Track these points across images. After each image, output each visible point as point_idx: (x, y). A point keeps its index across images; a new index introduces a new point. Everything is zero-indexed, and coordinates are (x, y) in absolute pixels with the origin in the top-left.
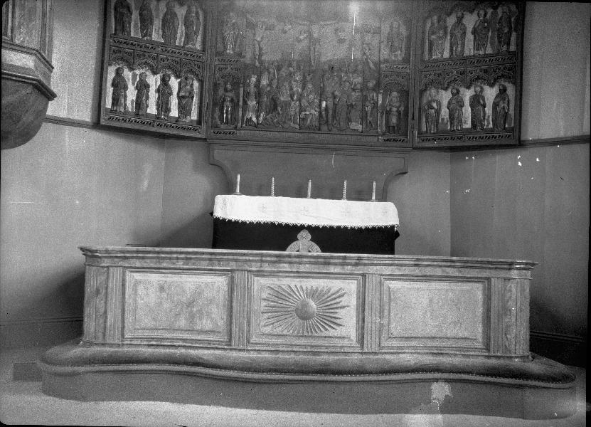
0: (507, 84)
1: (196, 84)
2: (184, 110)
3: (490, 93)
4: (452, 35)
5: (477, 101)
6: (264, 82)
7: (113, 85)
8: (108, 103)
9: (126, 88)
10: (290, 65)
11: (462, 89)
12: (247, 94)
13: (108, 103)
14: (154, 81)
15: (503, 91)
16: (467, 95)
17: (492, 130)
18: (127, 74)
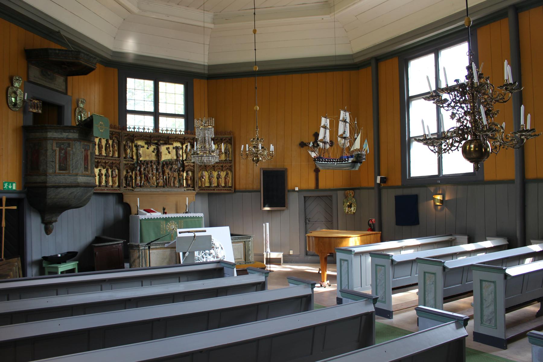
0: (229, 172)
1: (117, 171)
2: (113, 182)
3: (223, 174)
5: (219, 177)
6: (142, 169)
11: (213, 172)
12: (136, 174)
14: (104, 171)
15: (227, 174)
16: (215, 174)
17: (224, 187)
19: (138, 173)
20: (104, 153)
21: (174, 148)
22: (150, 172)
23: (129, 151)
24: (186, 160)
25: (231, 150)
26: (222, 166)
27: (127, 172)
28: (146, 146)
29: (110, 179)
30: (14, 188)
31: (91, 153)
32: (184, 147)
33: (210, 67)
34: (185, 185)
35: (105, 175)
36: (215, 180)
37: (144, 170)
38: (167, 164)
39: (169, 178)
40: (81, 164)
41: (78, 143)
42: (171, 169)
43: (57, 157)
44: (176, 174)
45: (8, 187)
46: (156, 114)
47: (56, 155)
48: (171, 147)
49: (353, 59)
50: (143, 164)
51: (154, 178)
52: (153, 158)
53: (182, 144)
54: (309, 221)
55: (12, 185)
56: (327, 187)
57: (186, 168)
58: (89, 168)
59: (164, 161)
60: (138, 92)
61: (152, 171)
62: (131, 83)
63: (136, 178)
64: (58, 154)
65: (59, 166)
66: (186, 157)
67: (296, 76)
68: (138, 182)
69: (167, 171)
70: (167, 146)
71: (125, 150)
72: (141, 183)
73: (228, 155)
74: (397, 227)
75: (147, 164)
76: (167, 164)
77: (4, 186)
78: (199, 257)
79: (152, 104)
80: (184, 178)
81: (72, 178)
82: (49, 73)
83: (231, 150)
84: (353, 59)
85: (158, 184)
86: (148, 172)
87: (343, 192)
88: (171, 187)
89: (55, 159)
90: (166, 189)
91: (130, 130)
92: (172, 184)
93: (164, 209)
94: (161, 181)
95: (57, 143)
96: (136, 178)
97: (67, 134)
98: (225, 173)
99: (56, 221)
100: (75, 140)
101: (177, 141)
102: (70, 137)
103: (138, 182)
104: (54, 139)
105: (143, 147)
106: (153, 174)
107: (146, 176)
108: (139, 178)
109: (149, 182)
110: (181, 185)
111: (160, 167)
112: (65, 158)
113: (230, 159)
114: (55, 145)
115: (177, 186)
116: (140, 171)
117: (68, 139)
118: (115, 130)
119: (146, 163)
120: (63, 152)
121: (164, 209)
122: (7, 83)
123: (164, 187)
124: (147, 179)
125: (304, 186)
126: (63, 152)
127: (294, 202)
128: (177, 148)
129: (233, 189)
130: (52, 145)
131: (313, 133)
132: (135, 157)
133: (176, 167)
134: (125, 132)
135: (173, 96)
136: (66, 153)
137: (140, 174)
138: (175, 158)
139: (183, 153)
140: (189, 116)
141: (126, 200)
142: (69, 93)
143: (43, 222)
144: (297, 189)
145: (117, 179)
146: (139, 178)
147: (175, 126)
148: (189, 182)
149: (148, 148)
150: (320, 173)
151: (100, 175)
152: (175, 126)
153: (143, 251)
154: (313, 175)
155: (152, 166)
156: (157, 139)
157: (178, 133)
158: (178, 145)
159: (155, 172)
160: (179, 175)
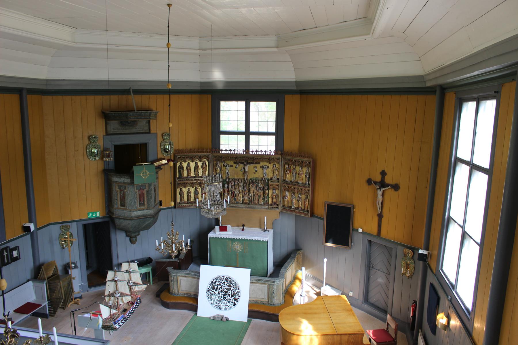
6: (230, 187)
8: (178, 201)
9: (184, 194)
10: (238, 180)
13: (178, 201)
14: (192, 190)
18: (184, 189)
19: (226, 189)
20: (192, 174)
23: (218, 170)
24: (272, 179)
30: (98, 215)
31: (147, 191)
32: (271, 166)
33: (297, 83)
34: (270, 202)
37: (232, 188)
38: (253, 182)
39: (254, 195)
40: (135, 202)
42: (256, 187)
43: (119, 196)
44: (261, 192)
45: (92, 216)
46: (247, 133)
49: (425, 82)
54: (373, 267)
57: (270, 187)
58: (146, 203)
59: (251, 179)
60: (231, 113)
62: (224, 105)
65: (121, 203)
66: (273, 175)
67: (371, 97)
69: (253, 189)
76: (253, 182)
77: (88, 215)
78: (216, 292)
80: (270, 195)
81: (128, 213)
84: (425, 82)
85: (243, 200)
86: (235, 189)
87: (403, 248)
88: (255, 204)
92: (256, 202)
93: (243, 226)
94: (246, 198)
99: (139, 234)
100: (128, 184)
101: (263, 161)
104: (116, 182)
105: (232, 166)
106: (239, 191)
107: (233, 193)
109: (235, 199)
110: (266, 203)
112: (124, 197)
115: (262, 203)
116: (228, 187)
117: (124, 183)
118: (203, 154)
120: (122, 192)
126: (122, 192)
127: (358, 243)
131: (381, 171)
133: (262, 186)
134: (215, 154)
135: (264, 114)
136: (124, 193)
137: (228, 191)
142: (153, 130)
143: (127, 236)
144: (360, 230)
147: (265, 145)
148: (274, 200)
150: (383, 219)
151: (189, 193)
152: (265, 145)
153: (175, 277)
154: (376, 219)
156: (247, 159)
160: (264, 193)
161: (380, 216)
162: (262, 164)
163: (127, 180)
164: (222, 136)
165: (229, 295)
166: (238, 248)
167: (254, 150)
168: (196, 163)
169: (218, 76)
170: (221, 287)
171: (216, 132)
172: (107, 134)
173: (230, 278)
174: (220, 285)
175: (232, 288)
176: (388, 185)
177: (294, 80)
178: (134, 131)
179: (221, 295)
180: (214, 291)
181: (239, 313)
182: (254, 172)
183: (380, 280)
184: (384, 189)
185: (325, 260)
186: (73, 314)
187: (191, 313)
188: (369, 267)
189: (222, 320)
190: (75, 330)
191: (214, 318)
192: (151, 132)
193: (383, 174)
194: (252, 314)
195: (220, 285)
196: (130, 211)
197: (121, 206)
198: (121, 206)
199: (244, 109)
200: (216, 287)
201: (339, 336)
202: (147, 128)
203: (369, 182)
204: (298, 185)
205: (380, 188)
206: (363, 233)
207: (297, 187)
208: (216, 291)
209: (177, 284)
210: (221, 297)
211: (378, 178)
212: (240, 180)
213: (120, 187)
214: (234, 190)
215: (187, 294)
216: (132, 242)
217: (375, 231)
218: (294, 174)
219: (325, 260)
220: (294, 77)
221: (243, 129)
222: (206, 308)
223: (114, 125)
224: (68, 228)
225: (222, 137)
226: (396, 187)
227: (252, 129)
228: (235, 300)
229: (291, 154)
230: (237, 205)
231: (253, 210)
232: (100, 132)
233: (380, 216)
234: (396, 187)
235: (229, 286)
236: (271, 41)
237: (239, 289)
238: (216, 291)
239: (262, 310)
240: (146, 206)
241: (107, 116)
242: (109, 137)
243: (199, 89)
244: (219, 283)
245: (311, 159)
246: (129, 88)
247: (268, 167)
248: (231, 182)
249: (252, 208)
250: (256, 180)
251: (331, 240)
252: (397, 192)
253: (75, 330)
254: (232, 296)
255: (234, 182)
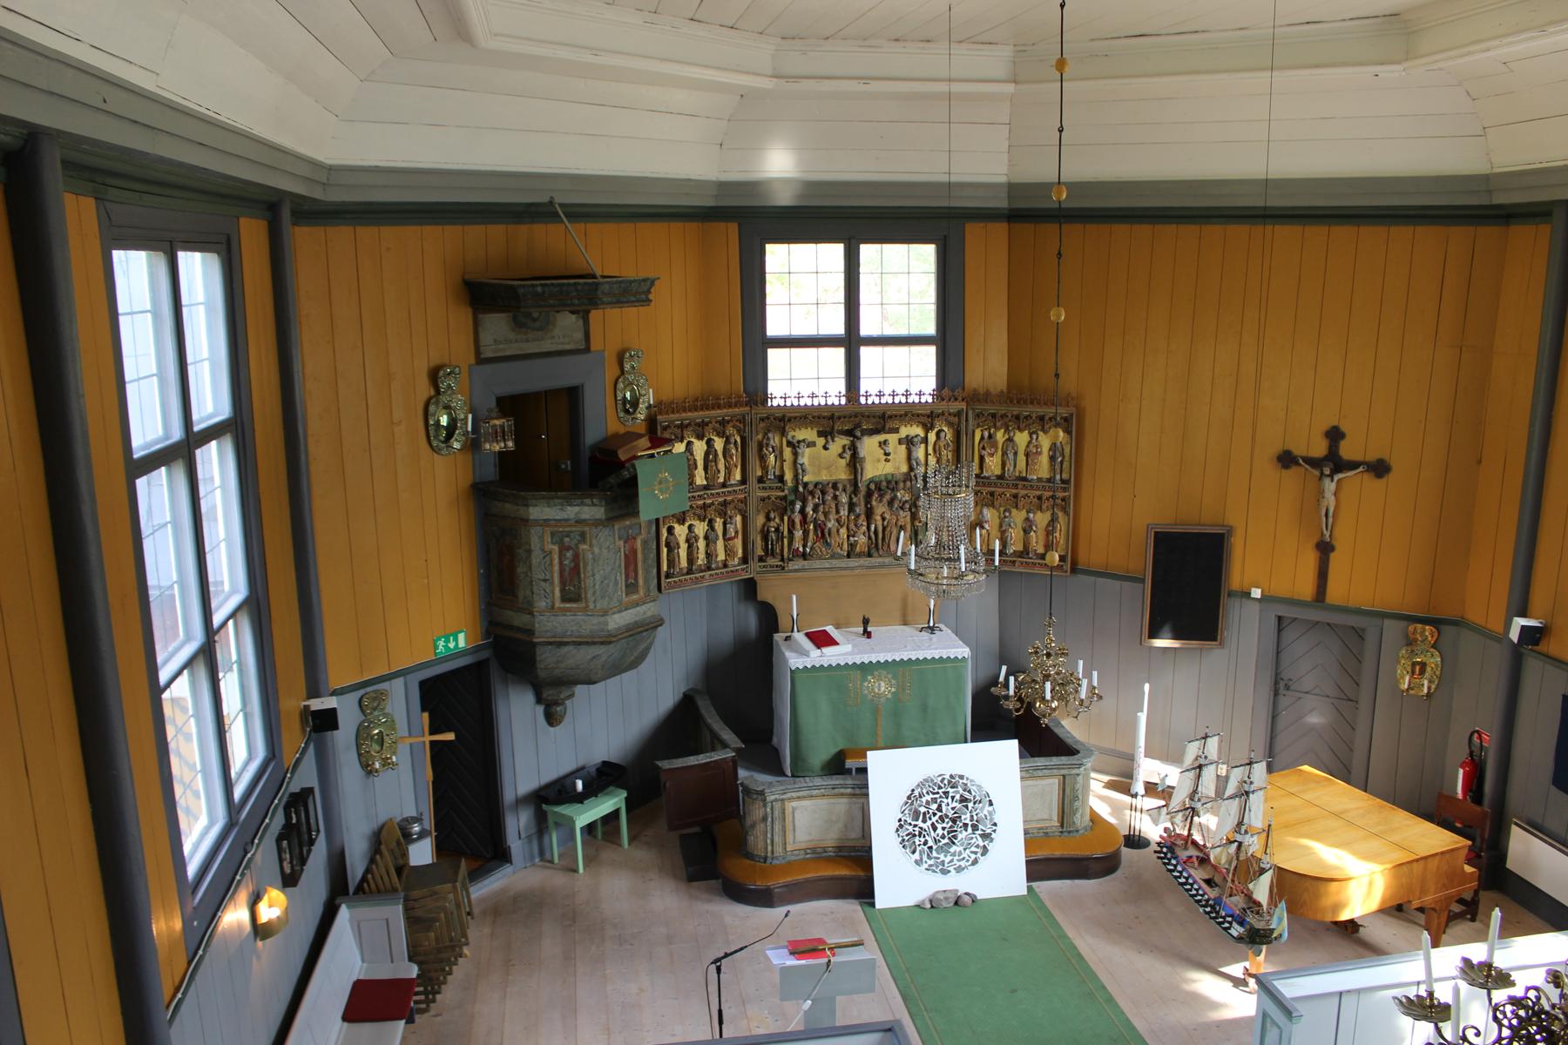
0: (1060, 514)
1: (739, 519)
2: (729, 552)
3: (1041, 519)
4: (1004, 454)
5: (1028, 528)
6: (809, 510)
7: (668, 545)
11: (1014, 511)
12: (792, 523)
14: (701, 528)
15: (1053, 520)
19: (797, 518)
21: (900, 442)
22: (833, 516)
25: (1067, 451)
26: (1039, 498)
27: (768, 519)
28: (821, 441)
29: (720, 544)
32: (932, 437)
33: (1013, 188)
35: (706, 538)
36: (1015, 535)
37: (815, 510)
40: (616, 583)
41: (604, 533)
42: (890, 503)
43: (556, 568)
45: (446, 647)
46: (851, 341)
47: (551, 564)
48: (892, 438)
49: (1490, 192)
50: (812, 493)
51: (843, 531)
52: (842, 474)
53: (927, 429)
54: (1287, 688)
55: (456, 640)
56: (1352, 604)
58: (641, 582)
59: (871, 481)
61: (838, 512)
62: (777, 256)
63: (790, 532)
64: (556, 561)
65: (562, 590)
68: (798, 545)
69: (880, 509)
70: (882, 437)
71: (763, 459)
72: (805, 546)
73: (1058, 467)
74: (1553, 788)
75: (823, 493)
77: (436, 647)
78: (924, 826)
79: (840, 312)
81: (595, 620)
82: (536, 315)
83: (1067, 451)
84: (1490, 192)
85: (852, 546)
86: (826, 514)
87: (1403, 624)
89: (552, 573)
90: (875, 561)
91: (775, 403)
93: (866, 622)
94: (862, 539)
95: (553, 534)
96: (790, 532)
97: (577, 509)
98: (1047, 516)
100: (597, 523)
102: (584, 516)
103: (798, 545)
104: (546, 523)
105: (812, 444)
106: (838, 521)
108: (798, 534)
109: (828, 545)
111: (860, 500)
112: (576, 570)
113: (1065, 476)
114: (548, 538)
116: (803, 511)
117: (579, 522)
119: (822, 488)
120: (569, 554)
121: (866, 622)
122: (424, 390)
123: (870, 555)
124: (822, 534)
125: (1282, 589)
126: (569, 554)
127: (1245, 628)
128: (909, 442)
129: (1068, 566)
130: (541, 538)
132: (788, 477)
133: (907, 497)
134: (760, 412)
135: (902, 279)
136: (576, 556)
137: (804, 521)
138: (904, 469)
139: (927, 455)
140: (949, 340)
141: (764, 594)
142: (596, 344)
143: (539, 700)
144: (1256, 593)
145: (738, 543)
146: (798, 534)
147: (903, 375)
149: (825, 448)
150: (1332, 556)
152: (903, 375)
153: (777, 806)
154: (1310, 558)
155: (835, 497)
156: (853, 420)
157: (914, 399)
158: (916, 430)
159: (844, 512)
161: (1325, 549)
162: (905, 431)
163: (592, 511)
164: (771, 352)
165: (966, 825)
166: (883, 687)
167: (874, 391)
168: (709, 443)
169: (779, 165)
170: (939, 809)
171: (756, 343)
172: (481, 360)
173: (961, 777)
174: (934, 801)
175: (970, 805)
176: (1353, 465)
177: (1003, 179)
178: (547, 346)
179: (940, 831)
180: (920, 823)
181: (1000, 873)
182: (881, 458)
183: (1314, 719)
184: (1341, 476)
185: (1147, 687)
186: (719, 970)
187: (851, 907)
188: (1279, 686)
189: (956, 903)
190: (721, 1022)
191: (934, 903)
192: (593, 348)
193: (1335, 435)
194: (1038, 869)
195: (934, 801)
196: (605, 613)
197: (564, 599)
198: (564, 599)
199: (842, 268)
200: (923, 810)
201: (1421, 863)
202: (580, 335)
203: (1287, 459)
204: (1025, 487)
205: (1331, 477)
206: (1264, 599)
207: (1023, 492)
208: (924, 821)
209: (784, 827)
210: (943, 837)
211: (1319, 449)
212: (840, 486)
213: (558, 537)
214: (822, 518)
215: (814, 850)
216: (552, 719)
217: (1306, 590)
218: (1011, 456)
219: (1147, 687)
220: (1003, 169)
221: (838, 328)
222: (900, 880)
223: (496, 326)
224: (380, 697)
225: (774, 355)
226: (1379, 469)
227: (867, 328)
228: (986, 836)
229: (986, 397)
230: (835, 563)
231: (884, 571)
232: (462, 352)
233: (1325, 549)
234: (1379, 469)
235: (963, 800)
236: (995, 61)
237: (991, 804)
238: (924, 821)
239: (1057, 854)
240: (642, 592)
241: (482, 295)
242: (487, 368)
243: (711, 203)
244: (928, 798)
245: (1073, 410)
246: (545, 199)
247: (925, 441)
248: (812, 493)
249: (882, 566)
250: (889, 482)
251: (1167, 629)
252: (1384, 480)
253: (721, 1022)
254: (975, 828)
255: (823, 493)
